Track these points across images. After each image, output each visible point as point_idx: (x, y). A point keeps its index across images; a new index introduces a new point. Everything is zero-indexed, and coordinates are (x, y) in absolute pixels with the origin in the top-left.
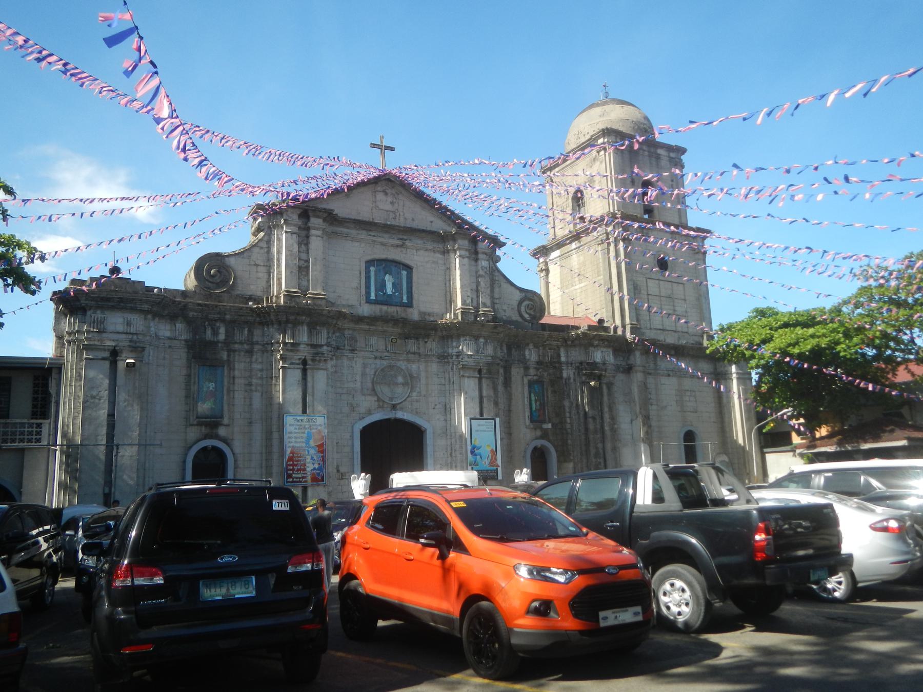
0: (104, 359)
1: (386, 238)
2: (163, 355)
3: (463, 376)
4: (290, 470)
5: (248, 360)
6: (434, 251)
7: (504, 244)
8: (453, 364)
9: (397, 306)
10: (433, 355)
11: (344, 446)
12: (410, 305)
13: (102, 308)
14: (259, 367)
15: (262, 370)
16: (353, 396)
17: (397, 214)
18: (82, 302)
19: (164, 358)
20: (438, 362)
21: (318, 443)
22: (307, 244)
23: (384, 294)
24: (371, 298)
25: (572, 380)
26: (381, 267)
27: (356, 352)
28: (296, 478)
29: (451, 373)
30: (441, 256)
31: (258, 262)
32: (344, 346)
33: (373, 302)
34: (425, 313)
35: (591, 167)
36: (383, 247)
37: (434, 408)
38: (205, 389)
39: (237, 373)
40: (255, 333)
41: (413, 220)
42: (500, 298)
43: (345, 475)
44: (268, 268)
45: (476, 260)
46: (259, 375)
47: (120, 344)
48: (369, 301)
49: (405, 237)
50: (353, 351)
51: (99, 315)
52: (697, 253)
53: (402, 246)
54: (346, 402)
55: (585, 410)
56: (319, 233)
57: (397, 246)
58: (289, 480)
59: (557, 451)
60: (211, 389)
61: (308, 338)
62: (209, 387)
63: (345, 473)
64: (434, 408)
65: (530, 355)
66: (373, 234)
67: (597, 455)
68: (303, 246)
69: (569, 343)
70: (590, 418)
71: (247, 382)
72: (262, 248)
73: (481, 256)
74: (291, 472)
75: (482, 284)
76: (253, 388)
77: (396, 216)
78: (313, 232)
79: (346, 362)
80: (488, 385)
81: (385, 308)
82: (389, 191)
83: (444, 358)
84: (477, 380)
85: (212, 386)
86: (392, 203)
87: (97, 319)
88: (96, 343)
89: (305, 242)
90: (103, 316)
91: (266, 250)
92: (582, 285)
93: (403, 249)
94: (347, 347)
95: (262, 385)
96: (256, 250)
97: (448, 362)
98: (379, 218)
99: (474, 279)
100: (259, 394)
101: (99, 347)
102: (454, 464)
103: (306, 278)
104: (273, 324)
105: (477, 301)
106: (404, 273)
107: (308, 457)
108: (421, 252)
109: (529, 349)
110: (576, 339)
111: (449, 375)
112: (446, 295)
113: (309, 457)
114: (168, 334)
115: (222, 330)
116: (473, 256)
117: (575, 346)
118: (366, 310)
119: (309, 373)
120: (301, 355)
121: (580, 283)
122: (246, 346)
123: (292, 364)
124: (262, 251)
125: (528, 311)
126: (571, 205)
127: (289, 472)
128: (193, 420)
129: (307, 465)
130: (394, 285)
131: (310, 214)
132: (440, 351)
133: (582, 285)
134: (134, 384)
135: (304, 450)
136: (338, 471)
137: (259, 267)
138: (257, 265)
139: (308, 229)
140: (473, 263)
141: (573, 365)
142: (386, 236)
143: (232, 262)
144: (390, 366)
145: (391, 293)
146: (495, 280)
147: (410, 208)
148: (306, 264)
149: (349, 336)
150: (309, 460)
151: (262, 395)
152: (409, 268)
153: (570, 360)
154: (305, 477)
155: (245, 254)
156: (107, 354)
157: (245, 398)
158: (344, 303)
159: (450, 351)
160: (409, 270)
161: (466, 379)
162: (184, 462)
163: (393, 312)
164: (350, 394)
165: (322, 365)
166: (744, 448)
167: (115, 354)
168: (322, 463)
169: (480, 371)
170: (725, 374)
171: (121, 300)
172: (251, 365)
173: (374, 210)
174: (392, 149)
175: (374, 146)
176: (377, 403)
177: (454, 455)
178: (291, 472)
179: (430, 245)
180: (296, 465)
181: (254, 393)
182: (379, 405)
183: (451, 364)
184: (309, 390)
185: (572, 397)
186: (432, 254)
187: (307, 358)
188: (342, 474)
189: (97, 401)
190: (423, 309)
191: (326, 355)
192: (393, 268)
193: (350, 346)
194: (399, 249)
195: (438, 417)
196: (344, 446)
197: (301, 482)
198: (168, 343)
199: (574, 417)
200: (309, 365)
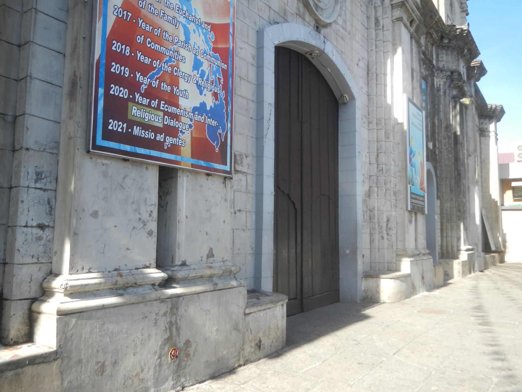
3: (400, 19)
4: (119, 80)
21: (216, 21)
25: (442, 93)
28: (146, 127)
29: (380, 10)
52: (464, 11)
55: (455, 133)
58: (114, 125)
69: (446, 41)
74: (123, 93)
102: (382, 179)
107: (183, 52)
110: (456, 36)
111: (376, 12)
113: (188, 56)
117: (447, 48)
127: (115, 90)
129: (183, 85)
135: (175, 22)
150: (186, 67)
153: (441, 65)
154: (172, 132)
166: (497, 202)
168: (222, 94)
170: (485, 131)
177: (383, 158)
178: (123, 93)
180: (146, 70)
185: (442, 115)
197: (158, 146)
199: (443, 141)
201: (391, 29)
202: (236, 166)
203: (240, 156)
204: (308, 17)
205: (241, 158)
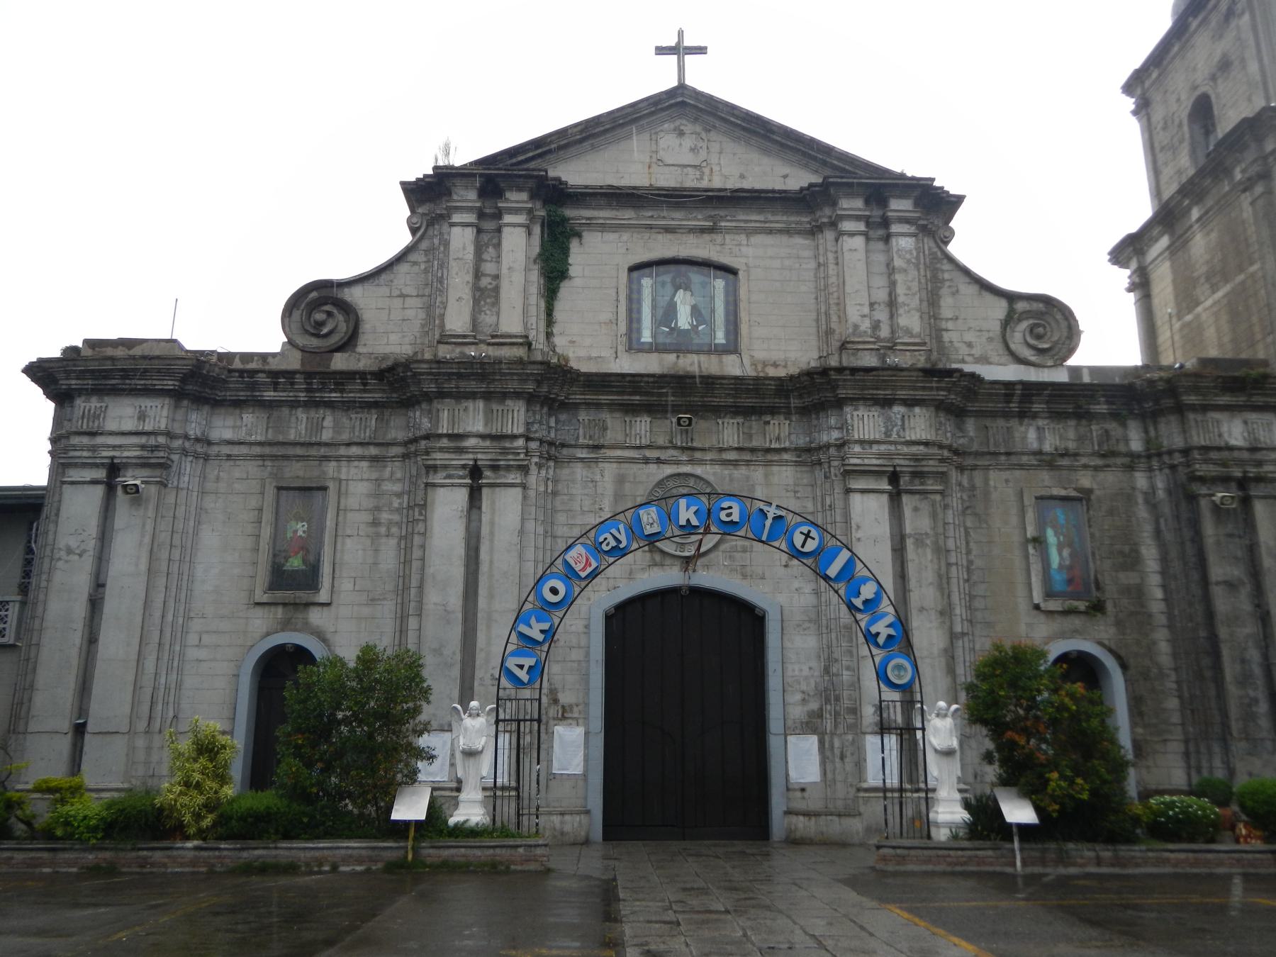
0: (94, 482)
1: (677, 217)
2: (216, 472)
3: (848, 491)
5: (375, 475)
6: (787, 232)
7: (957, 201)
8: (829, 467)
9: (698, 352)
10: (785, 450)
12: (732, 348)
13: (99, 391)
14: (397, 487)
15: (399, 495)
17: (707, 171)
18: (61, 382)
19: (218, 479)
20: (798, 464)
22: (498, 246)
23: (672, 329)
24: (643, 340)
26: (667, 278)
27: (603, 451)
30: (807, 242)
31: (407, 291)
32: (578, 438)
33: (647, 347)
34: (765, 364)
35: (1221, 37)
36: (669, 236)
37: (786, 566)
38: (289, 535)
39: (352, 502)
40: (392, 424)
41: (742, 177)
42: (957, 319)
43: (571, 711)
44: (425, 299)
45: (887, 239)
46: (396, 505)
47: (126, 454)
48: (634, 345)
49: (722, 213)
50: (597, 447)
51: (94, 403)
53: (712, 230)
56: (521, 219)
57: (703, 231)
59: (1124, 666)
60: (300, 533)
61: (486, 425)
62: (295, 532)
63: (571, 706)
64: (786, 566)
65: (1040, 439)
66: (650, 214)
67: (1245, 680)
68: (491, 249)
70: (1218, 583)
71: (370, 518)
72: (415, 263)
73: (895, 228)
75: (900, 290)
76: (383, 530)
77: (703, 174)
78: (508, 219)
79: (579, 471)
80: (916, 509)
81: (671, 358)
82: (688, 128)
83: (810, 456)
84: (885, 498)
85: (301, 528)
86: (692, 150)
87: (89, 411)
88: (85, 454)
89: (495, 241)
90: (98, 405)
91: (423, 267)
92: (1220, 294)
93: (714, 236)
94: (581, 441)
95: (399, 525)
96: (403, 268)
97: (820, 463)
98: (666, 179)
99: (880, 282)
100: (393, 542)
101: (85, 461)
103: (494, 309)
104: (419, 403)
105: (892, 326)
106: (719, 284)
108: (758, 239)
109: (1038, 428)
112: (817, 320)
114: (228, 435)
115: (328, 422)
116: (881, 232)
118: (627, 365)
119: (485, 491)
120: (467, 459)
121: (1214, 292)
122: (373, 451)
123: (449, 477)
124: (416, 268)
125: (1032, 342)
126: (1187, 136)
128: (260, 596)
130: (695, 311)
131: (502, 185)
132: (802, 441)
133: (1220, 294)
134: (144, 525)
136: (556, 701)
137: (408, 300)
138: (403, 296)
139: (498, 215)
140: (880, 245)
141: (1166, 458)
142: (678, 214)
143: (355, 296)
144: (679, 475)
145: (687, 327)
146: (944, 280)
147: (734, 154)
148: (494, 283)
149: (586, 418)
151: (399, 544)
152: (730, 271)
155: (384, 277)
156: (101, 474)
157: (364, 550)
158: (582, 353)
159: (825, 438)
160: (731, 277)
161: (856, 499)
162: (237, 676)
163: (692, 364)
165: (513, 478)
167: (114, 469)
169: (894, 477)
171: (126, 374)
172: (379, 485)
173: (655, 168)
174: (701, 50)
175: (660, 51)
176: (648, 555)
179: (780, 219)
181: (384, 540)
182: (653, 559)
183: (826, 466)
184: (485, 530)
186: (784, 239)
187: (479, 463)
188: (563, 707)
189: (76, 557)
190: (760, 355)
191: (522, 456)
192: (695, 276)
193: (591, 438)
194: (707, 237)
195: (796, 584)
198: (226, 450)
200: (488, 478)
201: (839, 504)
204: (668, 561)
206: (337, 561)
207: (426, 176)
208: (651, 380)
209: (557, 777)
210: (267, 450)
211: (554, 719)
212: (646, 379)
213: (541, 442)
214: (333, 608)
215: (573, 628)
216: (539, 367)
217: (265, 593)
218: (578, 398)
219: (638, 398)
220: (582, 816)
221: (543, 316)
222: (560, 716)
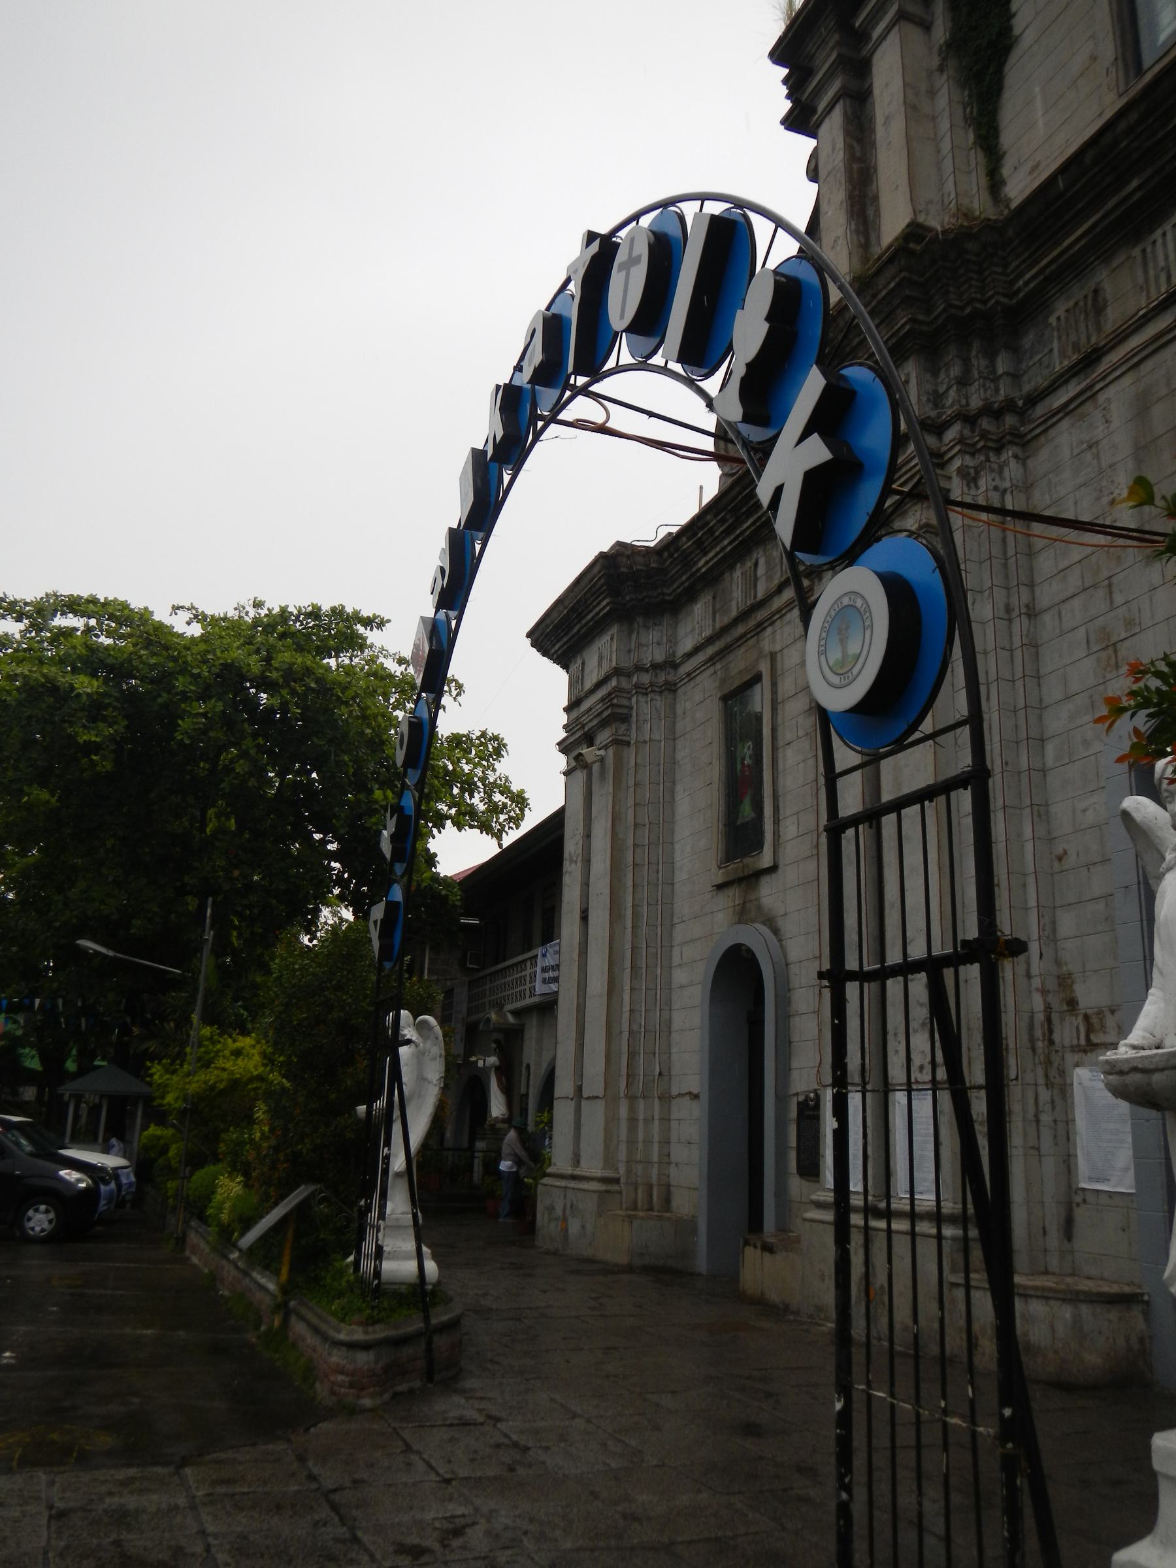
11: (1089, 866)
16: (1110, 586)
43: (1103, 1028)
54: (1081, 633)
63: (1100, 1013)
136: (1072, 1003)
164: (1094, 586)
188: (1086, 1017)
196: (1089, 866)
202: (1092, 1037)
203: (1098, 1014)
205: (1101, 1019)
206: (781, 791)
207: (785, 81)
208: (1134, 116)
209: (1090, 1198)
210: (710, 650)
211: (1076, 1049)
212: (1122, 125)
213: (969, 419)
214: (780, 870)
215: (1090, 818)
216: (891, 270)
217: (720, 868)
218: (1026, 281)
219: (1135, 183)
220: (1085, 1309)
221: (977, 158)
222: (1083, 1042)
